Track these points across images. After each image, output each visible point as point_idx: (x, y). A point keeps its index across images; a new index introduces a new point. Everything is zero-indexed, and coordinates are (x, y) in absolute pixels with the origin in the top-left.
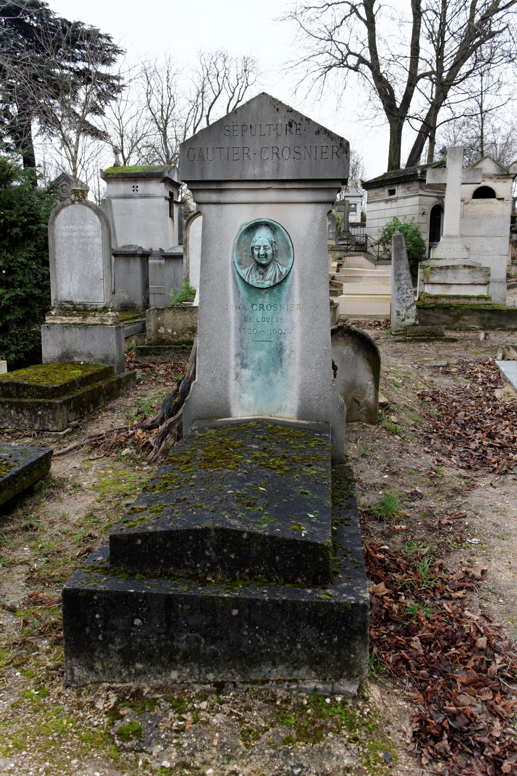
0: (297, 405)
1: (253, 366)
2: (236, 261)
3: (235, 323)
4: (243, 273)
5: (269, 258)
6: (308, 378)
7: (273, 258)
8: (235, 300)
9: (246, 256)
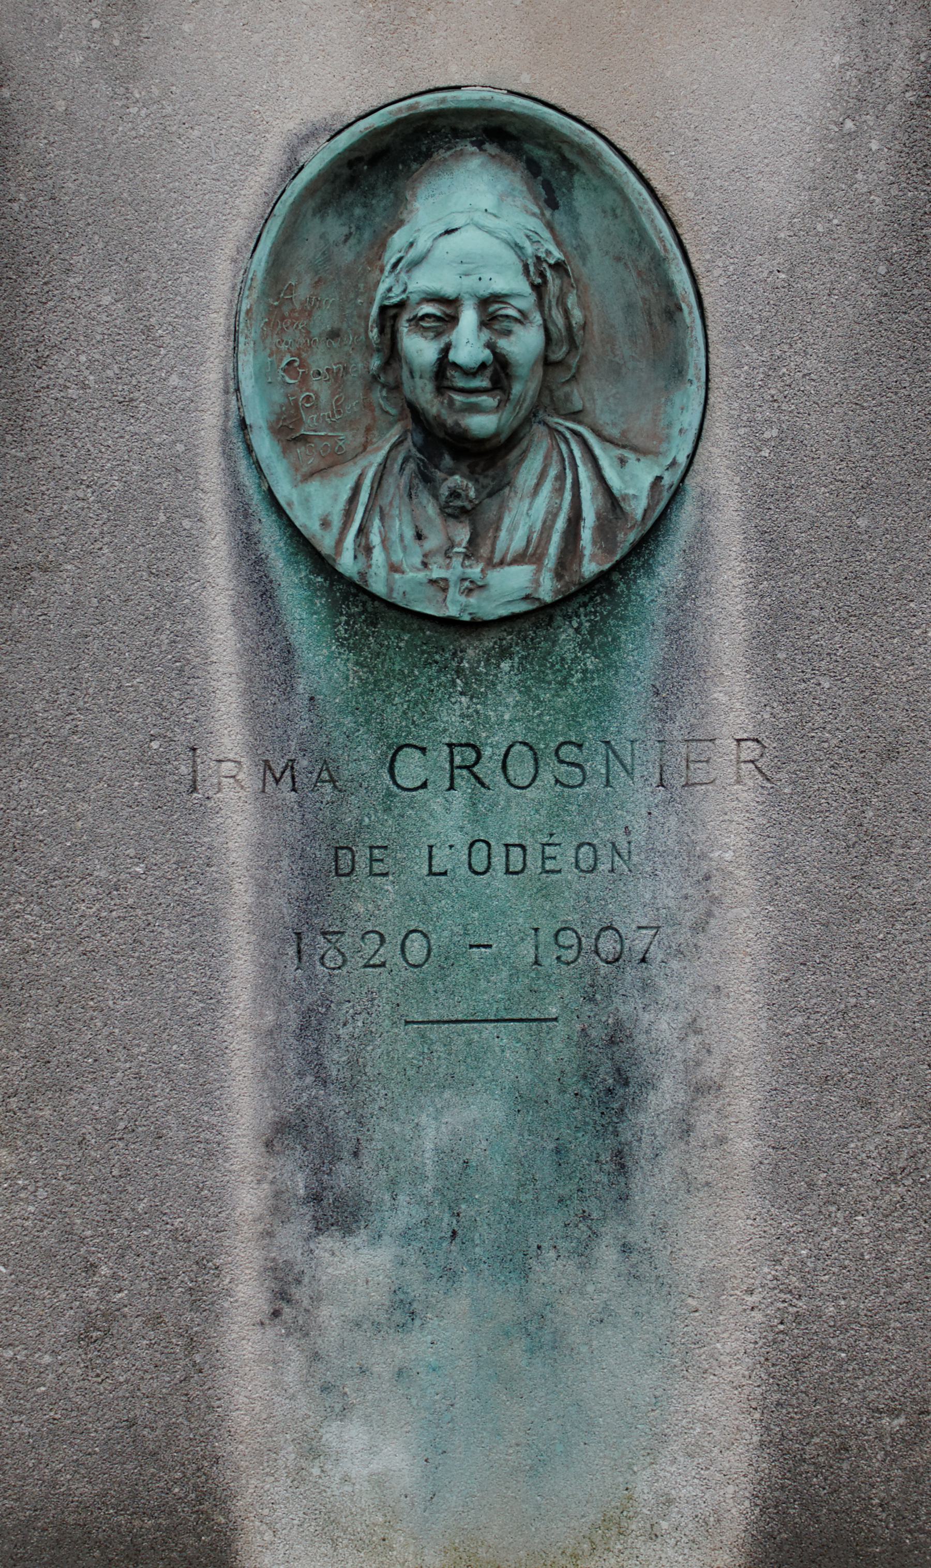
0: (746, 1488)
1: (405, 1213)
2: (257, 416)
3: (263, 888)
4: (317, 505)
5: (523, 388)
6: (826, 1283)
7: (545, 387)
8: (255, 714)
9: (337, 377)
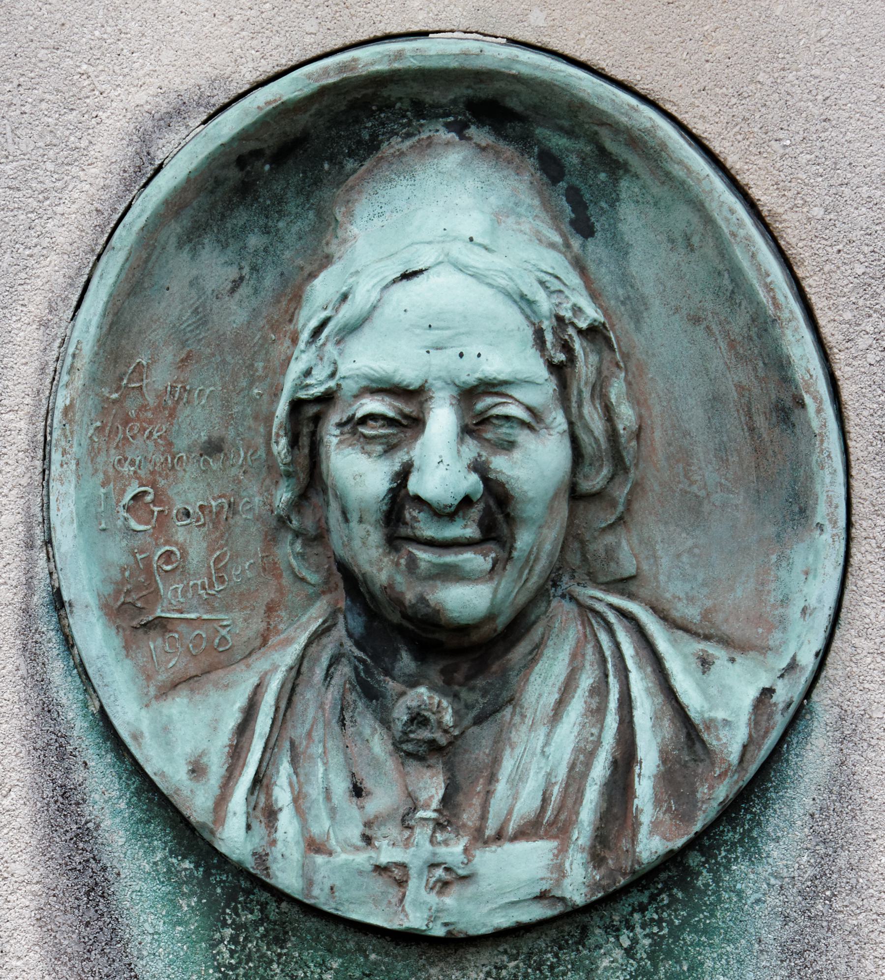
2: (82, 586)
4: (183, 736)
5: (536, 538)
7: (572, 536)
9: (218, 520)
